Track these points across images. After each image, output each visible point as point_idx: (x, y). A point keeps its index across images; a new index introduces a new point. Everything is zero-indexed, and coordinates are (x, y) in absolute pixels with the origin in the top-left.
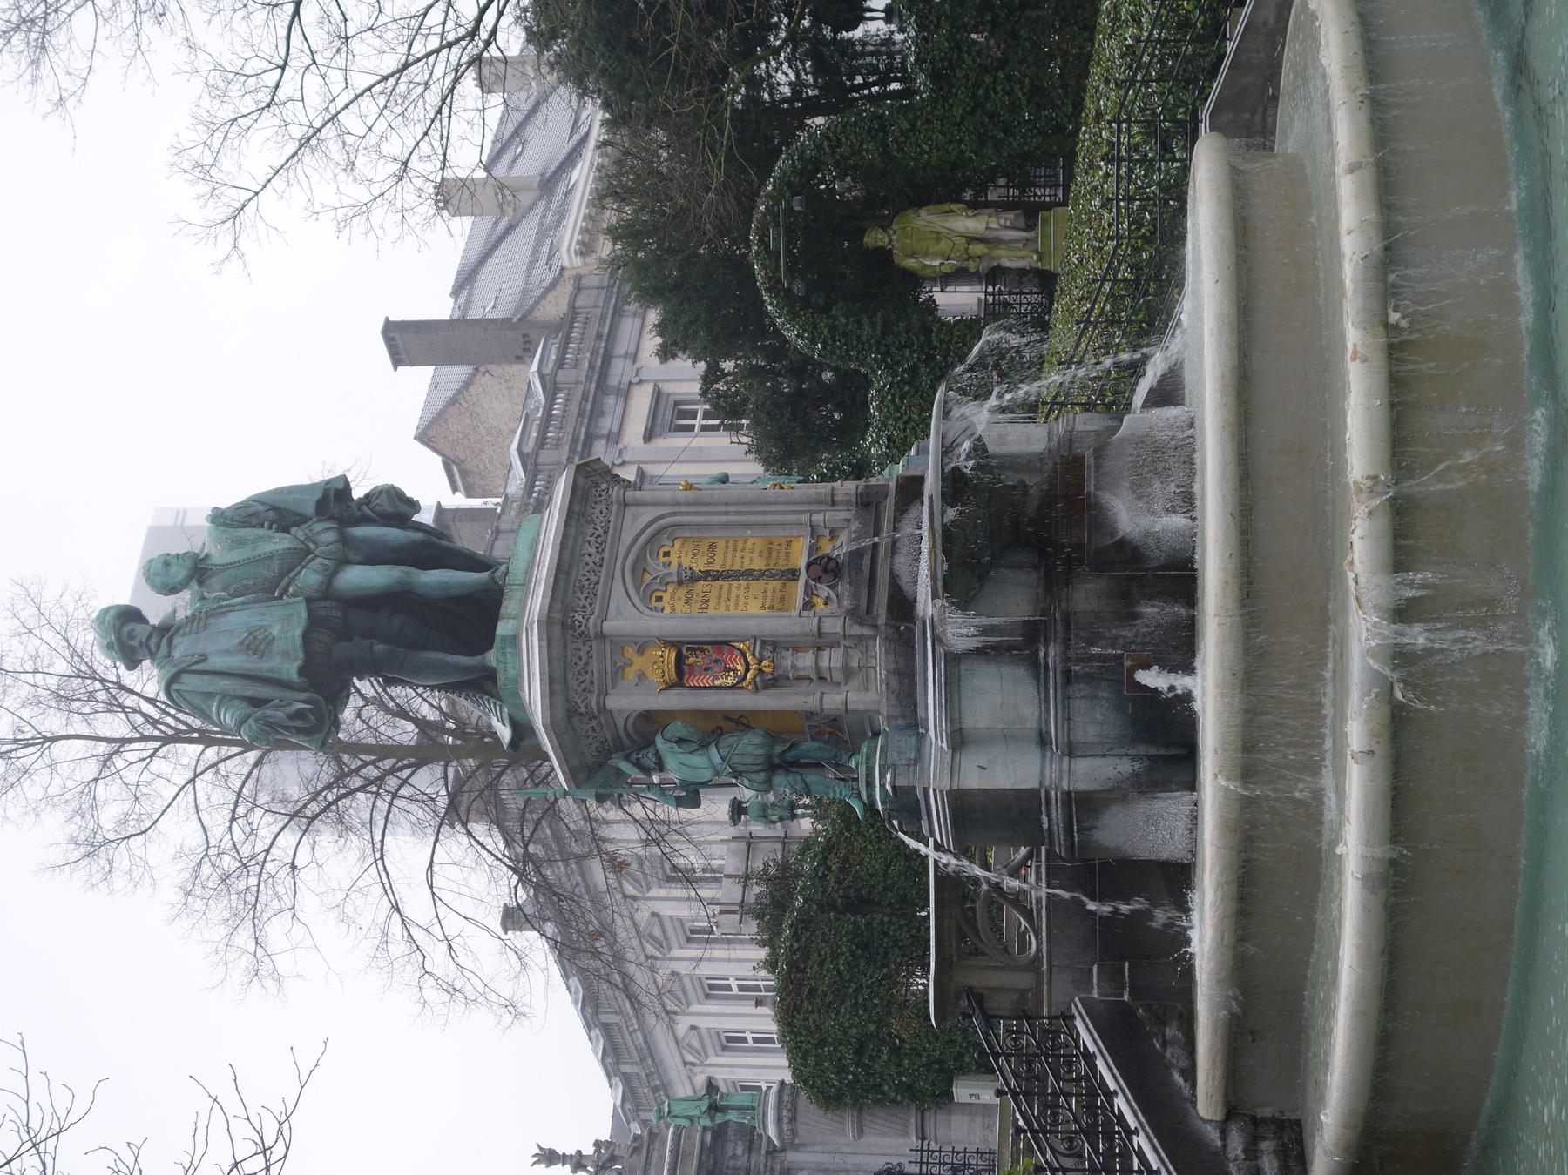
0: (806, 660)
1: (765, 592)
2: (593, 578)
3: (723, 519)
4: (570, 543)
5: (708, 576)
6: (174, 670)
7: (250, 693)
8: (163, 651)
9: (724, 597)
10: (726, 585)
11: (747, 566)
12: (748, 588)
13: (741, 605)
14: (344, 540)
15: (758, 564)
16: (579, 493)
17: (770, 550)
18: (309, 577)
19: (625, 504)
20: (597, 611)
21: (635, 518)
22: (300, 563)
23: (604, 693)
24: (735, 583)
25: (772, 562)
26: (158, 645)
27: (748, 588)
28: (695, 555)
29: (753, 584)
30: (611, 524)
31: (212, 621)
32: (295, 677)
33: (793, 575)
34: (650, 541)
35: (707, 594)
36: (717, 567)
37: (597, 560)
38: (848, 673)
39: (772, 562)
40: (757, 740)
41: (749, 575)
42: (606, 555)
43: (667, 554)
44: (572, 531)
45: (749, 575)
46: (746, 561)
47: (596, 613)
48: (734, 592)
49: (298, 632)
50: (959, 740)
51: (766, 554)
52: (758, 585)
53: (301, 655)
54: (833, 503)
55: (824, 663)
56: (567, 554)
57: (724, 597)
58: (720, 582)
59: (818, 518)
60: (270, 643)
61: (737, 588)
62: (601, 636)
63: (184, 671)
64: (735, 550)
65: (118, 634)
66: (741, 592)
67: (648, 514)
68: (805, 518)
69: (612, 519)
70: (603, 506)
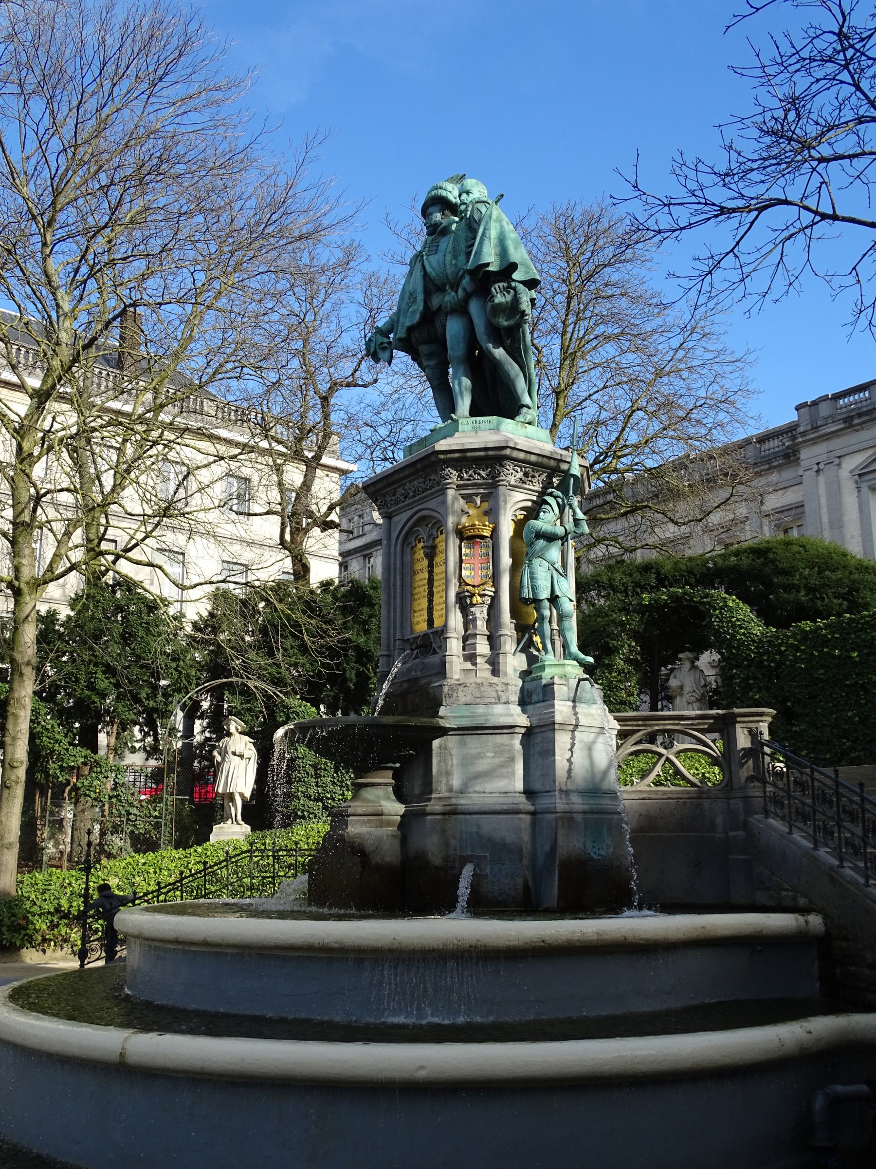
4: (401, 475)
11: (435, 590)
12: (424, 597)
16: (426, 462)
24: (427, 587)
29: (426, 599)
30: (433, 490)
44: (407, 472)
56: (396, 477)
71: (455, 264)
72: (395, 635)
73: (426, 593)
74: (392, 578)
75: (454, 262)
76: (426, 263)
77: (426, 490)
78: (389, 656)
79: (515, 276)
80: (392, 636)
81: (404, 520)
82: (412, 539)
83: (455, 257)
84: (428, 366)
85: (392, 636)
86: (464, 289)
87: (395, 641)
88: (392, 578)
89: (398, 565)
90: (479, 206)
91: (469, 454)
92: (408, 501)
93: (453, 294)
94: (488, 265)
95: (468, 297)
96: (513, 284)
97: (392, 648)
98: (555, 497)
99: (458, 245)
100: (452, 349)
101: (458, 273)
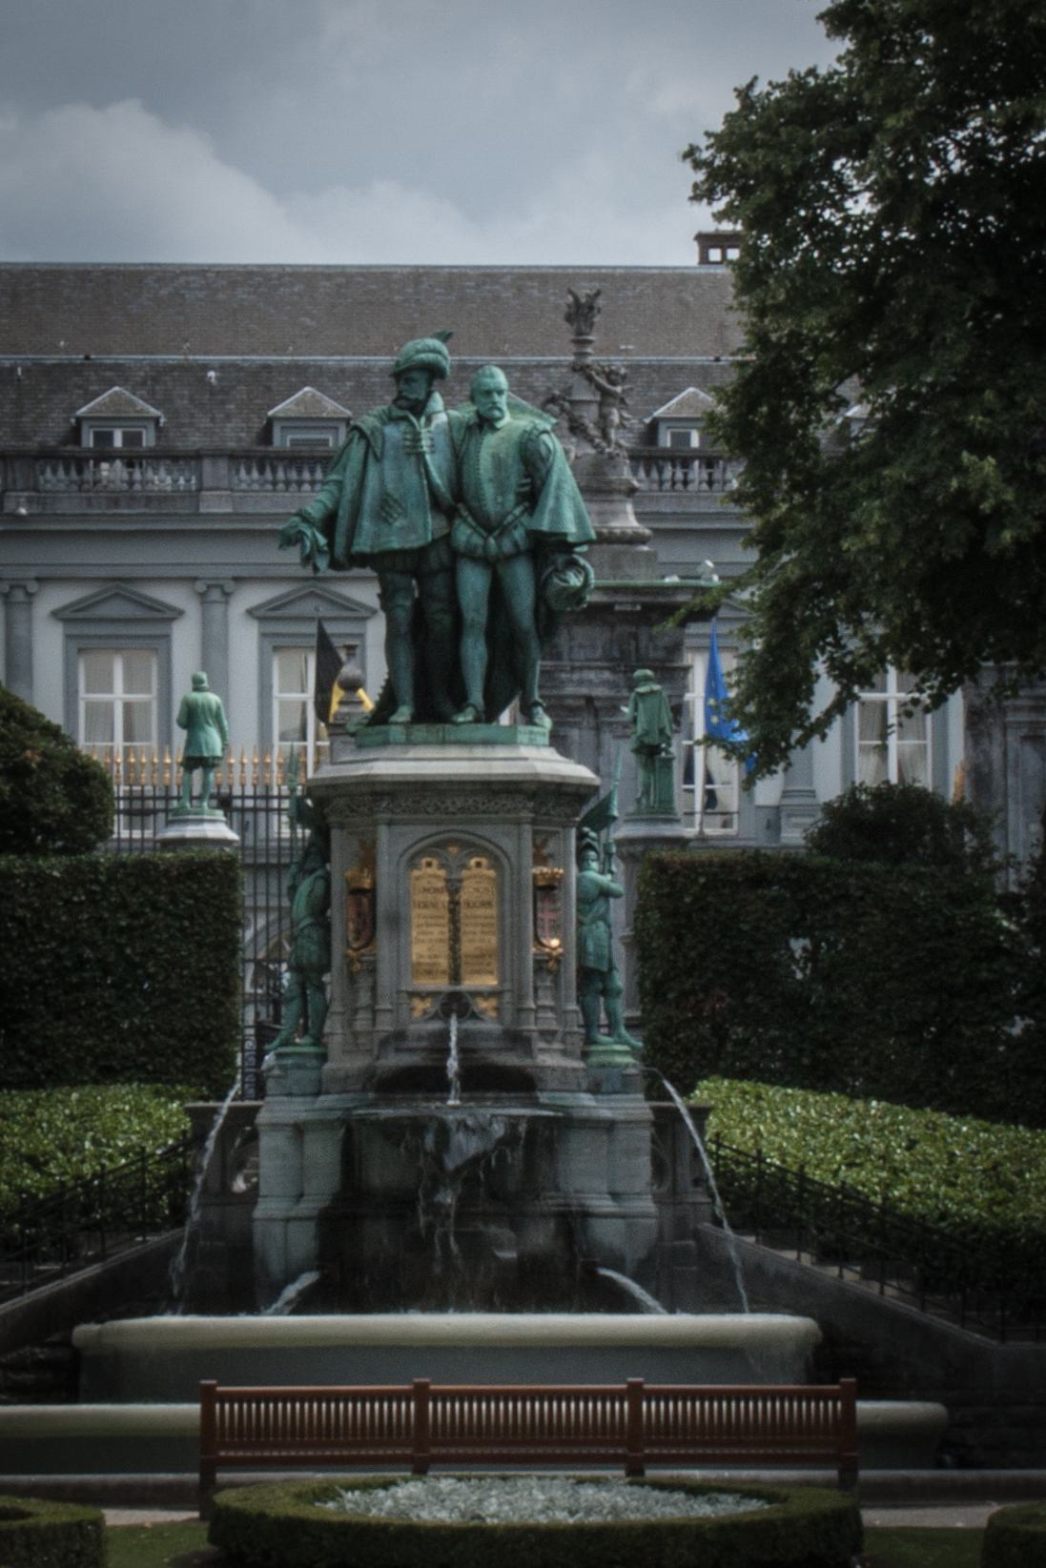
0: (364, 999)
1: (436, 956)
2: (429, 809)
3: (508, 914)
5: (454, 907)
6: (368, 433)
7: (341, 513)
8: (397, 413)
10: (445, 921)
11: (464, 939)
13: (421, 937)
14: (509, 559)
15: (467, 947)
17: (483, 956)
18: (465, 534)
19: (518, 823)
20: (400, 817)
22: (479, 524)
23: (342, 826)
24: (446, 930)
25: (469, 960)
26: (401, 408)
27: (441, 941)
30: (493, 816)
31: (413, 459)
32: (356, 548)
33: (455, 977)
34: (486, 849)
35: (435, 905)
36: (464, 912)
37: (451, 809)
38: (356, 1035)
39: (469, 960)
40: (314, 959)
41: (455, 938)
43: (478, 865)
45: (455, 938)
46: (470, 937)
47: (396, 817)
49: (396, 545)
50: (299, 1130)
51: (477, 953)
52: (443, 950)
53: (376, 550)
54: (520, 1010)
55: (361, 1015)
58: (447, 915)
59: (507, 997)
60: (385, 520)
61: (440, 932)
62: (375, 824)
63: (368, 446)
64: (483, 925)
65: (409, 369)
67: (508, 844)
68: (507, 986)
69: (501, 815)
71: (502, 504)
75: (500, 500)
77: (484, 812)
78: (390, 1011)
81: (421, 835)
83: (501, 489)
84: (401, 606)
86: (516, 544)
91: (564, 789)
92: (437, 816)
93: (492, 541)
94: (565, 535)
95: (518, 553)
96: (582, 561)
99: (508, 478)
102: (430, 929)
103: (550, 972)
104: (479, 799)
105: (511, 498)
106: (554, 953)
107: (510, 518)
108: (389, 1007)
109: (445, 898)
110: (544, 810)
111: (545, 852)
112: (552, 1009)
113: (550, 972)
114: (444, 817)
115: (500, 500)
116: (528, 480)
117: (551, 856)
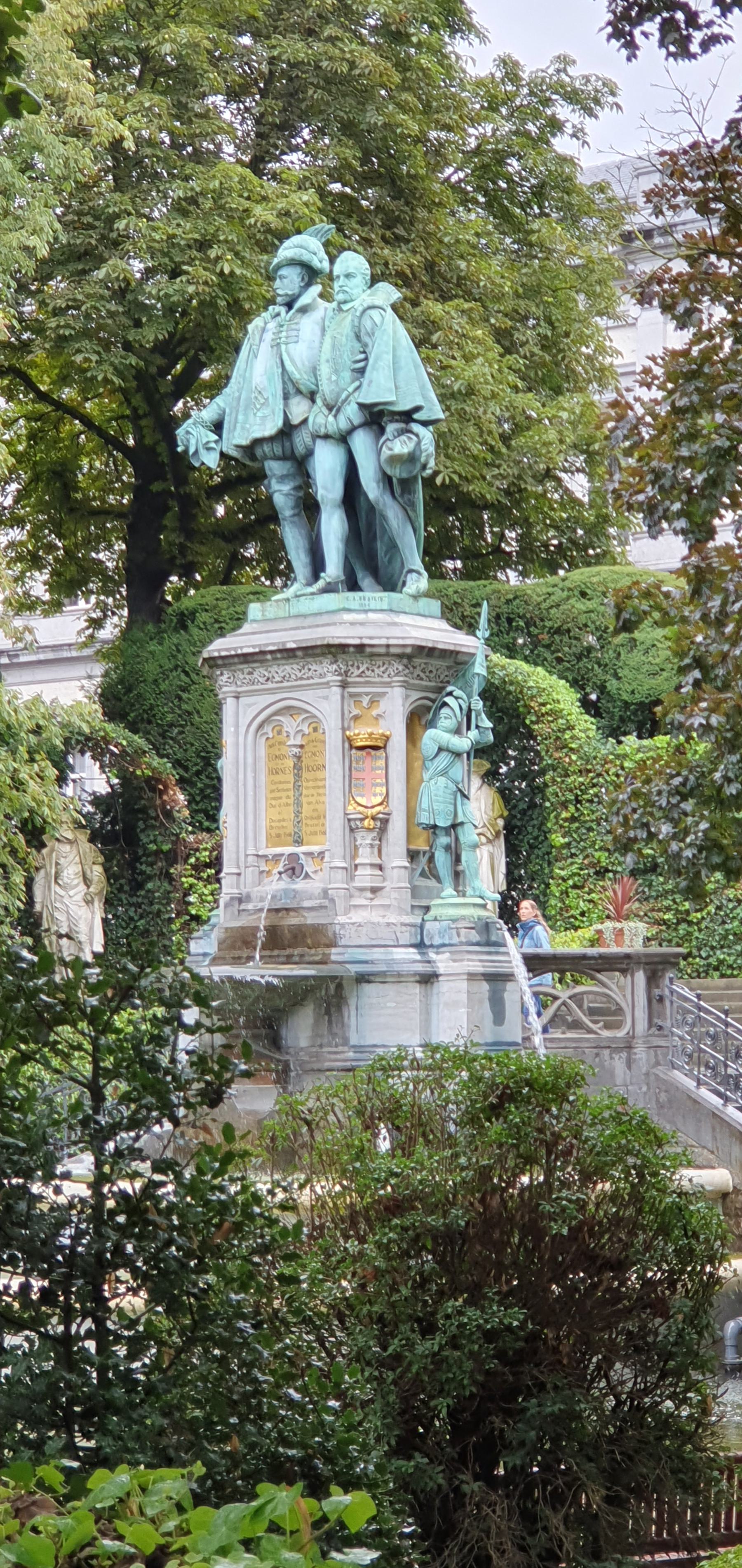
2: (262, 680)
9: (281, 786)
10: (291, 786)
11: (304, 800)
12: (288, 805)
15: (306, 810)
21: (326, 698)
28: (314, 754)
29: (291, 808)
30: (311, 681)
36: (305, 775)
37: (278, 679)
39: (309, 822)
42: (285, 684)
45: (298, 804)
46: (311, 799)
48: (284, 794)
51: (315, 814)
57: (281, 786)
66: (284, 800)
70: (320, 671)
71: (336, 382)
72: (246, 849)
73: (291, 801)
74: (241, 776)
75: (334, 378)
76: (285, 357)
77: (301, 679)
78: (239, 874)
79: (416, 416)
80: (242, 850)
82: (268, 729)
85: (242, 850)
87: (247, 856)
88: (241, 776)
89: (250, 760)
90: (374, 313)
92: (270, 685)
93: (331, 418)
97: (242, 864)
98: (456, 698)
99: (341, 356)
100: (325, 488)
101: (338, 395)
102: (278, 795)
103: (369, 830)
104: (295, 666)
105: (347, 375)
106: (370, 812)
107: (344, 396)
108: (236, 871)
109: (290, 763)
110: (357, 672)
111: (374, 713)
112: (372, 865)
113: (369, 830)
114: (275, 685)
115: (334, 378)
116: (362, 356)
117: (378, 717)
